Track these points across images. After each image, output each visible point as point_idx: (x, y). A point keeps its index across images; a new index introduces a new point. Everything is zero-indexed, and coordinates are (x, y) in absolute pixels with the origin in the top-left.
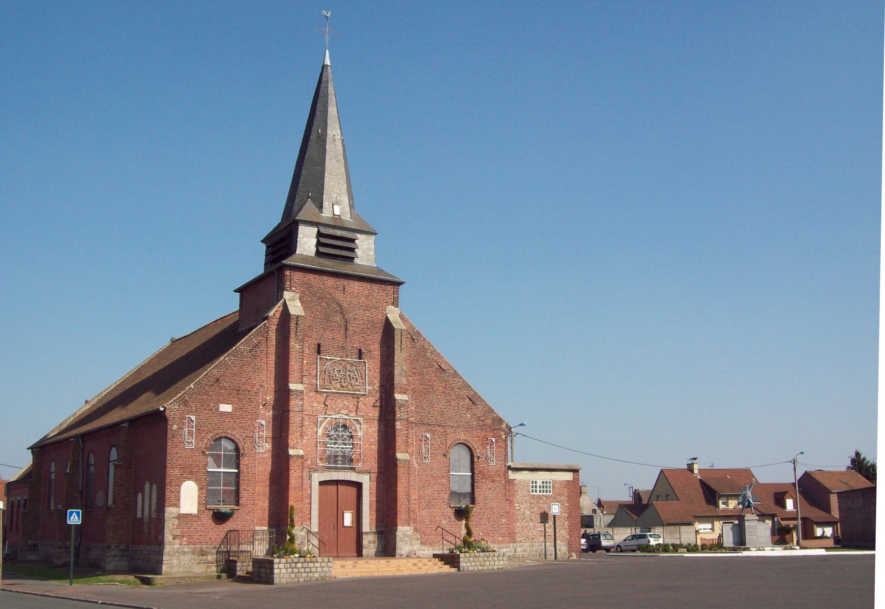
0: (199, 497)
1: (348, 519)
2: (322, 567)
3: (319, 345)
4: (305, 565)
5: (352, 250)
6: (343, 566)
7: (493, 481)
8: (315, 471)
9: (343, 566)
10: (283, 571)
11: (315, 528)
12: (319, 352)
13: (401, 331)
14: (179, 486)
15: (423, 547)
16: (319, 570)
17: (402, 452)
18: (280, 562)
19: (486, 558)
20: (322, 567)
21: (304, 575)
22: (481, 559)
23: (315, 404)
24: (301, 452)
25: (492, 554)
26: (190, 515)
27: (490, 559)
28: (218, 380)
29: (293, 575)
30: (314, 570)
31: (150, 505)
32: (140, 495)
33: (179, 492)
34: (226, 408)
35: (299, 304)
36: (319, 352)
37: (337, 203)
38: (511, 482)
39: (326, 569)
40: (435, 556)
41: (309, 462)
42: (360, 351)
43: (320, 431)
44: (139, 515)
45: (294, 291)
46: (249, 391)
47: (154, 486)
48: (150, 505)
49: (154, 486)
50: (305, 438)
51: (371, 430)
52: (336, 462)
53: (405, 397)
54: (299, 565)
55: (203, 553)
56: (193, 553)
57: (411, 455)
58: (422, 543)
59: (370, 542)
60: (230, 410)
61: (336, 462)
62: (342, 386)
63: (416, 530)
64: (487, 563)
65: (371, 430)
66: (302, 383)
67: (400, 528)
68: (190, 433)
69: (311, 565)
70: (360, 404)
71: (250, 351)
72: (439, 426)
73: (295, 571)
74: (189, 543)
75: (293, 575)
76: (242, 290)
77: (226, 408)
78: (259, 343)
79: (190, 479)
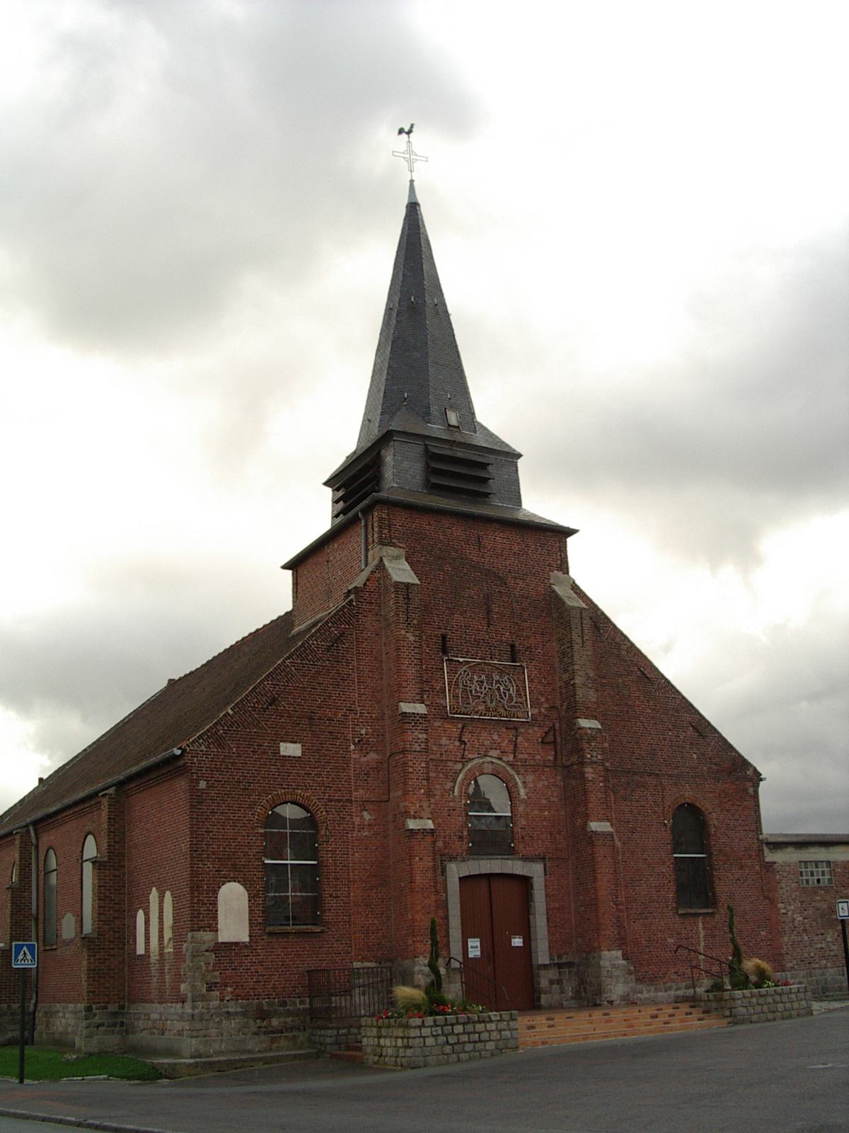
0: (251, 911)
3: (444, 637)
4: (469, 1028)
5: (485, 481)
8: (452, 859)
10: (430, 1041)
12: (445, 651)
13: (582, 610)
14: (215, 892)
16: (495, 1035)
18: (423, 1025)
22: (770, 1000)
23: (444, 741)
24: (430, 825)
26: (237, 944)
30: (485, 1036)
31: (161, 930)
32: (141, 914)
33: (215, 904)
34: (291, 749)
35: (407, 567)
37: (452, 407)
39: (508, 1033)
40: (678, 1000)
42: (512, 646)
44: (140, 950)
47: (168, 894)
48: (161, 930)
49: (168, 894)
50: (433, 800)
51: (540, 785)
53: (595, 724)
55: (263, 1015)
56: (244, 1014)
58: (638, 980)
59: (551, 982)
62: (487, 709)
63: (625, 956)
65: (540, 785)
67: (605, 953)
69: (480, 1027)
70: (520, 739)
71: (329, 649)
72: (650, 775)
73: (452, 1040)
74: (236, 997)
76: (294, 565)
77: (291, 749)
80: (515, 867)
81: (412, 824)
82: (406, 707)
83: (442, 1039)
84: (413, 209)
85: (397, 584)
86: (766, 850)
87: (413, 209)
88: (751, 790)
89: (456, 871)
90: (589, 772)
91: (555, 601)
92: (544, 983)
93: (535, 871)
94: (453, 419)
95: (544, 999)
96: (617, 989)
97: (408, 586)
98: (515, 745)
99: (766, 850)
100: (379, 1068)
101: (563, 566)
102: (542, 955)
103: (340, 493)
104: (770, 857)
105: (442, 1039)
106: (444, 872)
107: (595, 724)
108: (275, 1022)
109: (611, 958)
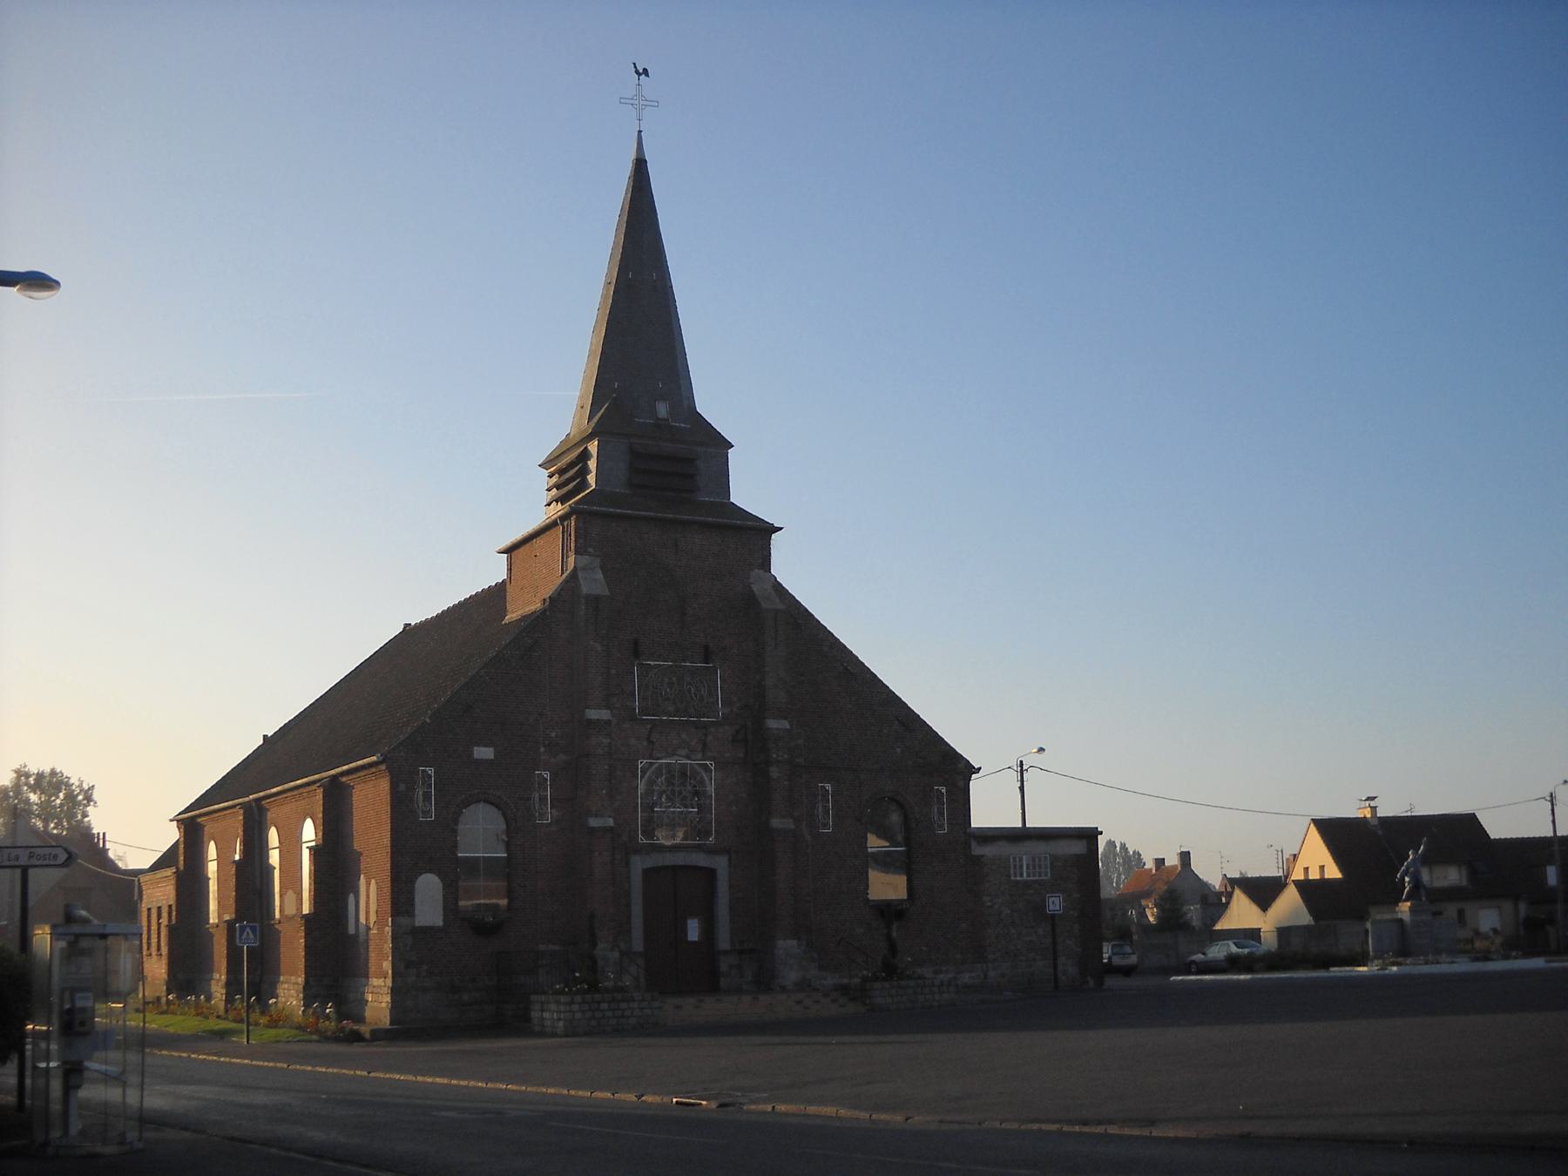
1: (693, 931)
3: (636, 642)
6: (678, 1007)
10: (578, 1015)
11: (638, 944)
18: (572, 1002)
23: (633, 741)
24: (610, 822)
26: (432, 928)
30: (628, 1013)
32: (351, 898)
34: (484, 753)
35: (600, 576)
39: (648, 1012)
43: (641, 787)
44: (352, 930)
45: (590, 554)
53: (785, 724)
54: (604, 1006)
66: (608, 707)
68: (427, 796)
69: (624, 1005)
70: (710, 738)
73: (598, 1015)
75: (594, 1023)
76: (509, 551)
77: (484, 753)
79: (430, 871)
80: (700, 860)
81: (594, 822)
82: (593, 714)
83: (589, 1014)
84: (640, 166)
85: (587, 597)
86: (974, 844)
87: (640, 166)
88: (961, 784)
89: (639, 864)
90: (774, 772)
91: (751, 600)
92: (723, 967)
93: (721, 863)
94: (662, 410)
95: (723, 982)
96: (791, 976)
97: (597, 598)
98: (705, 745)
99: (974, 844)
100: (542, 1034)
101: (766, 563)
102: (724, 941)
103: (555, 479)
104: (977, 850)
105: (589, 1014)
106: (627, 863)
107: (785, 724)
108: (466, 997)
109: (786, 946)
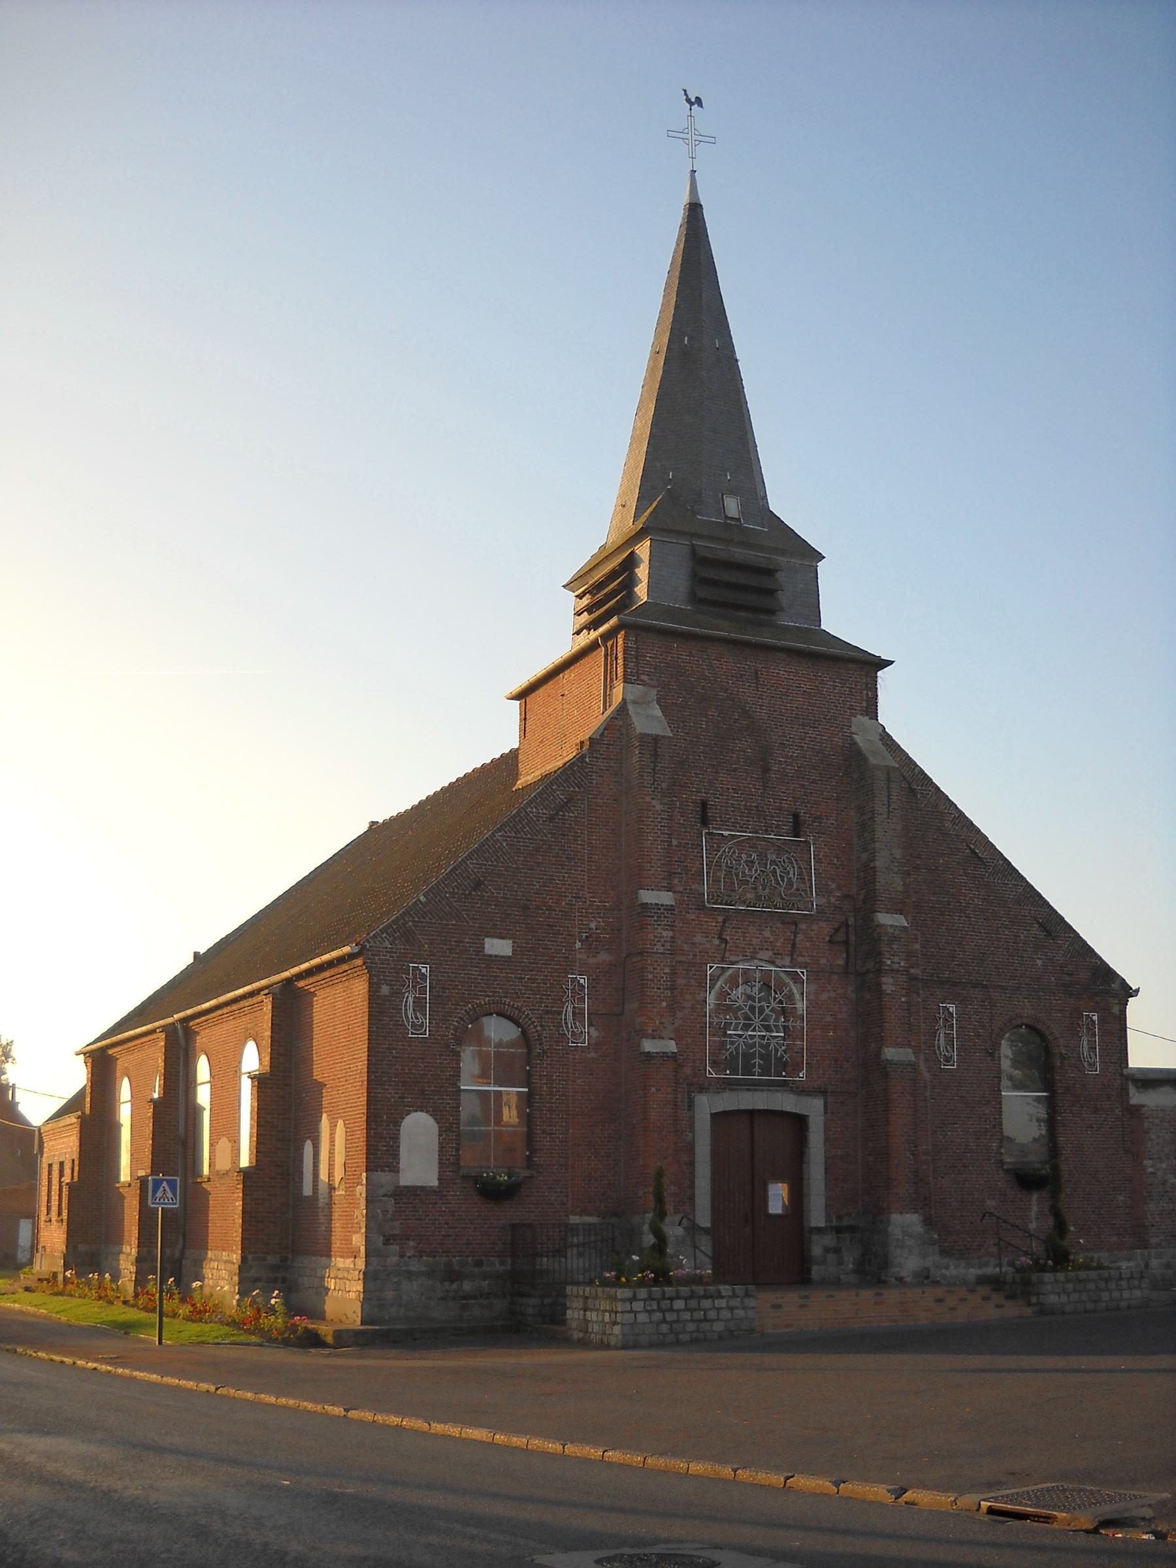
0: (442, 1148)
1: (778, 1196)
2: (732, 1309)
3: (704, 804)
4: (693, 1303)
5: (771, 593)
6: (777, 1307)
7: (1096, 1111)
8: (702, 1089)
9: (777, 1307)
10: (642, 1318)
11: (704, 1219)
12: (705, 821)
13: (888, 770)
14: (397, 1124)
15: (946, 1260)
16: (726, 1314)
17: (898, 1045)
18: (634, 1298)
19: (1102, 1284)
20: (732, 1309)
21: (691, 1327)
22: (1092, 1286)
23: (699, 938)
24: (672, 1046)
25: (1093, 1274)
26: (423, 1188)
27: (1112, 1286)
28: (478, 884)
29: (665, 1328)
30: (712, 1314)
32: (308, 1147)
33: (396, 1138)
34: (498, 947)
35: (658, 712)
36: (705, 821)
37: (732, 492)
38: (1135, 1112)
39: (740, 1313)
40: (982, 1280)
41: (688, 1070)
42: (796, 816)
43: (711, 1000)
44: (307, 1191)
45: (643, 683)
46: (550, 909)
47: (340, 1123)
49: (340, 1123)
50: (679, 1014)
51: (825, 996)
52: (748, 1070)
54: (679, 1304)
55: (452, 1276)
56: (430, 1274)
57: (916, 1053)
58: (944, 1252)
59: (827, 1250)
60: (508, 952)
61: (748, 1070)
62: (758, 898)
63: (928, 1221)
64: (1105, 1296)
65: (825, 996)
66: (670, 889)
67: (896, 1217)
68: (419, 1004)
69: (707, 1303)
70: (800, 937)
71: (551, 819)
72: (975, 986)
73: (670, 1317)
74: (421, 1253)
75: (665, 1328)
76: (522, 695)
77: (498, 947)
78: (569, 800)
79: (421, 1109)
80: (786, 1102)
81: (649, 1046)
82: (648, 897)
83: (657, 1316)
84: (694, 211)
85: (643, 736)
86: (1132, 1090)
87: (694, 211)
88: (1116, 1010)
89: (706, 1105)
90: (888, 984)
91: (854, 757)
92: (816, 1251)
93: (814, 1108)
94: (732, 506)
95: (816, 1272)
96: (908, 1263)
97: (656, 739)
98: (794, 945)
99: (1132, 1090)
100: (585, 1344)
101: (871, 708)
102: (817, 1217)
103: (586, 601)
104: (1137, 1097)
105: (657, 1316)
106: (691, 1106)
107: (901, 921)
108: (467, 1286)
109: (904, 1223)
